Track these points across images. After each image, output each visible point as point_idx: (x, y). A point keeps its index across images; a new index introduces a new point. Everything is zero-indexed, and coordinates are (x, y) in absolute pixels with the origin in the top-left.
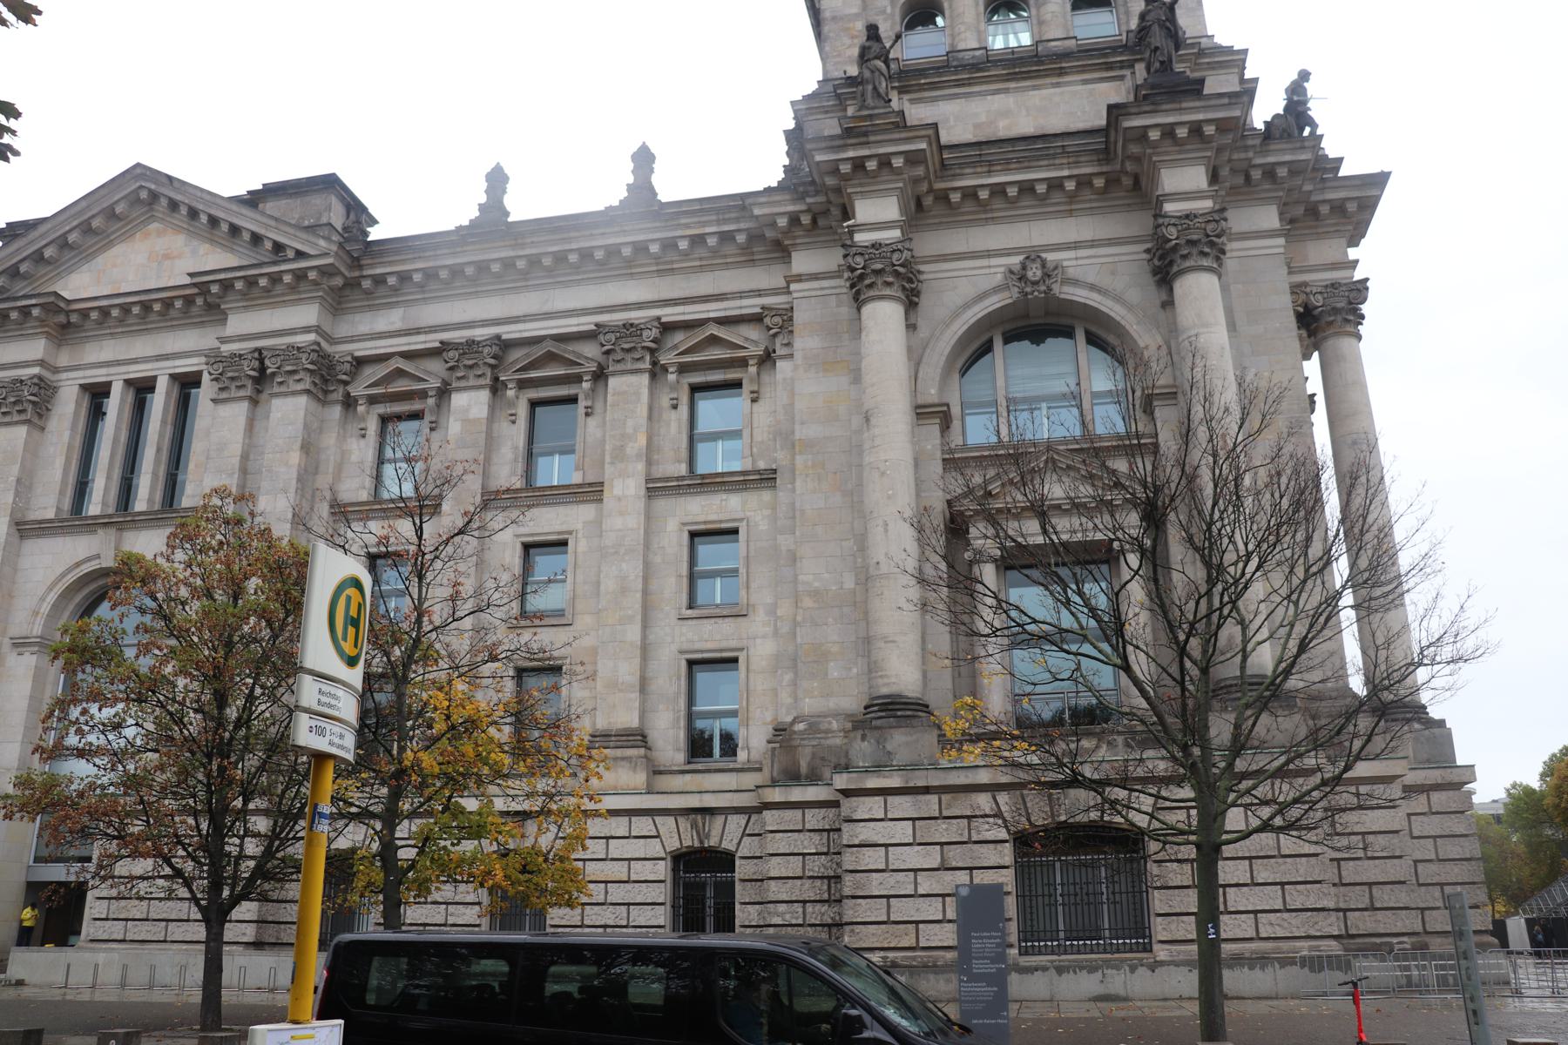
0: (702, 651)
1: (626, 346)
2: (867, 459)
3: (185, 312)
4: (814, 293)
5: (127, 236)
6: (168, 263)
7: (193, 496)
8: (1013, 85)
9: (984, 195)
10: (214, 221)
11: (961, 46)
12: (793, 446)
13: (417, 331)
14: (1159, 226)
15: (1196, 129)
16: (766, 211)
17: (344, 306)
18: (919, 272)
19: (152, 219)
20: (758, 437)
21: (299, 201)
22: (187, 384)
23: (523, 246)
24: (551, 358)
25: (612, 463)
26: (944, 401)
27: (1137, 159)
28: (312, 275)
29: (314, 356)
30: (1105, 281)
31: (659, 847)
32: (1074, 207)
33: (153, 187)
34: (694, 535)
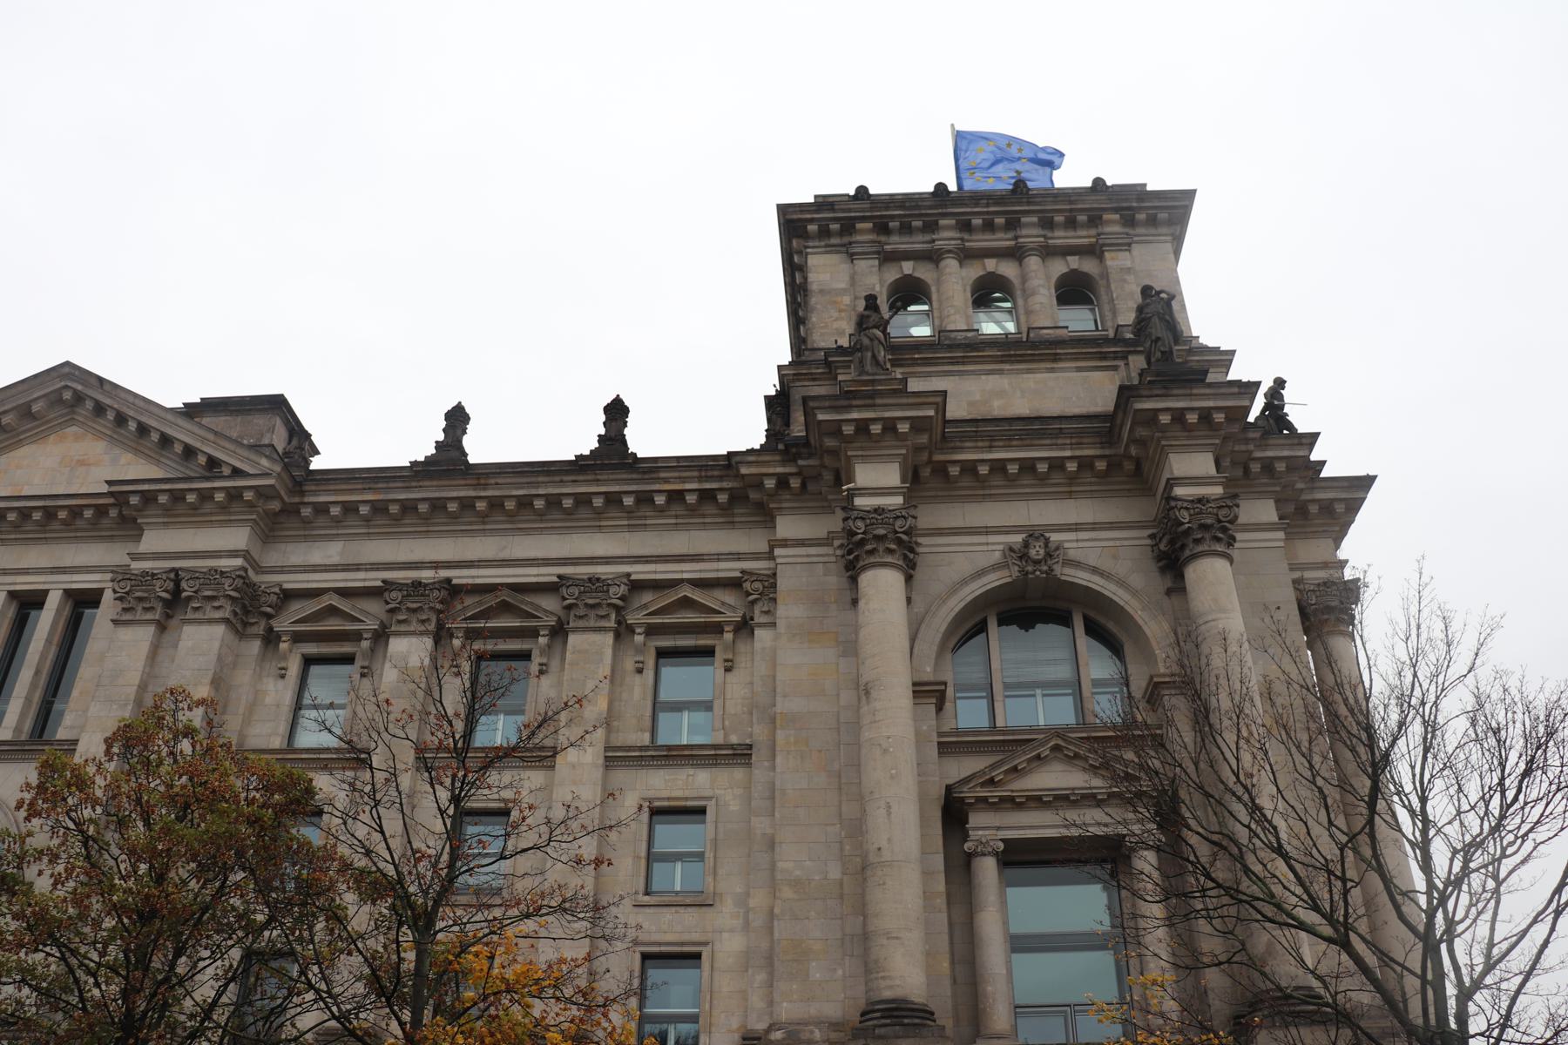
0: (660, 944)
1: (591, 601)
2: (866, 735)
3: (94, 524)
4: (799, 560)
5: (40, 437)
7: (72, 727)
8: (1007, 367)
9: (983, 470)
10: (143, 430)
11: (951, 327)
12: (773, 720)
13: (357, 568)
14: (1173, 508)
15: (1206, 415)
17: (276, 533)
18: (917, 543)
19: (71, 422)
20: (731, 709)
21: (239, 418)
22: (82, 602)
23: (485, 486)
24: (506, 608)
26: (943, 679)
27: (1142, 443)
28: (248, 496)
29: (239, 582)
30: (1106, 564)
32: (1074, 489)
33: (79, 387)
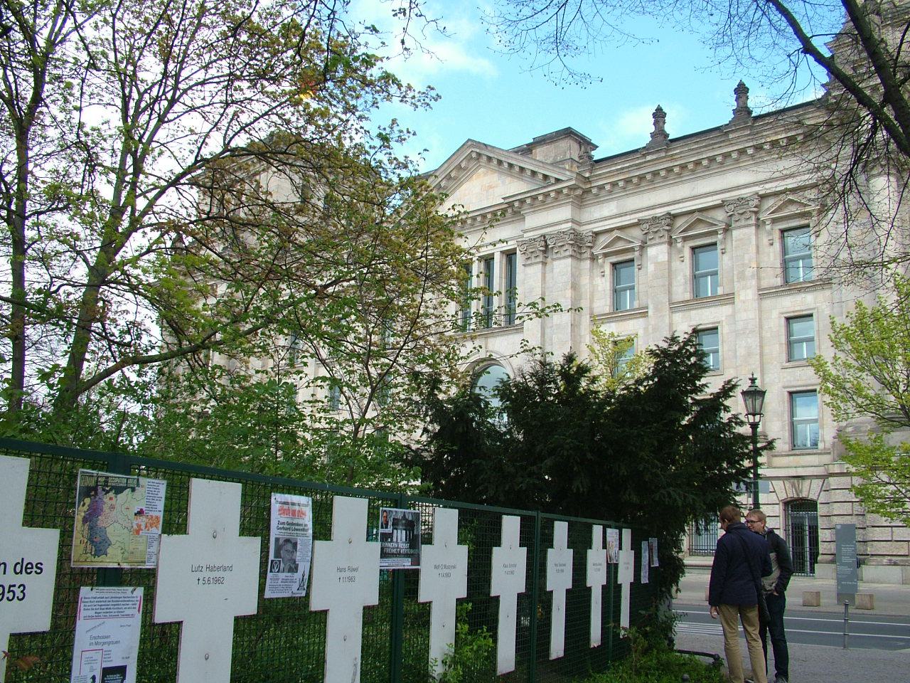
0: (796, 387)
5: (469, 178)
6: (491, 190)
16: (812, 122)
22: (510, 256)
23: (676, 160)
25: (738, 281)
29: (572, 236)
31: (775, 497)
33: (478, 151)
34: (788, 319)
